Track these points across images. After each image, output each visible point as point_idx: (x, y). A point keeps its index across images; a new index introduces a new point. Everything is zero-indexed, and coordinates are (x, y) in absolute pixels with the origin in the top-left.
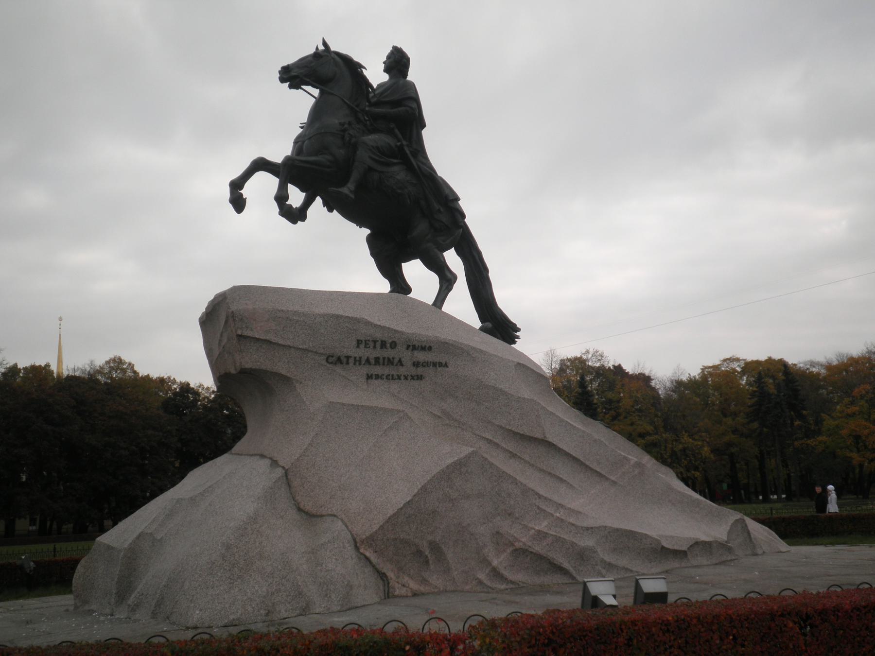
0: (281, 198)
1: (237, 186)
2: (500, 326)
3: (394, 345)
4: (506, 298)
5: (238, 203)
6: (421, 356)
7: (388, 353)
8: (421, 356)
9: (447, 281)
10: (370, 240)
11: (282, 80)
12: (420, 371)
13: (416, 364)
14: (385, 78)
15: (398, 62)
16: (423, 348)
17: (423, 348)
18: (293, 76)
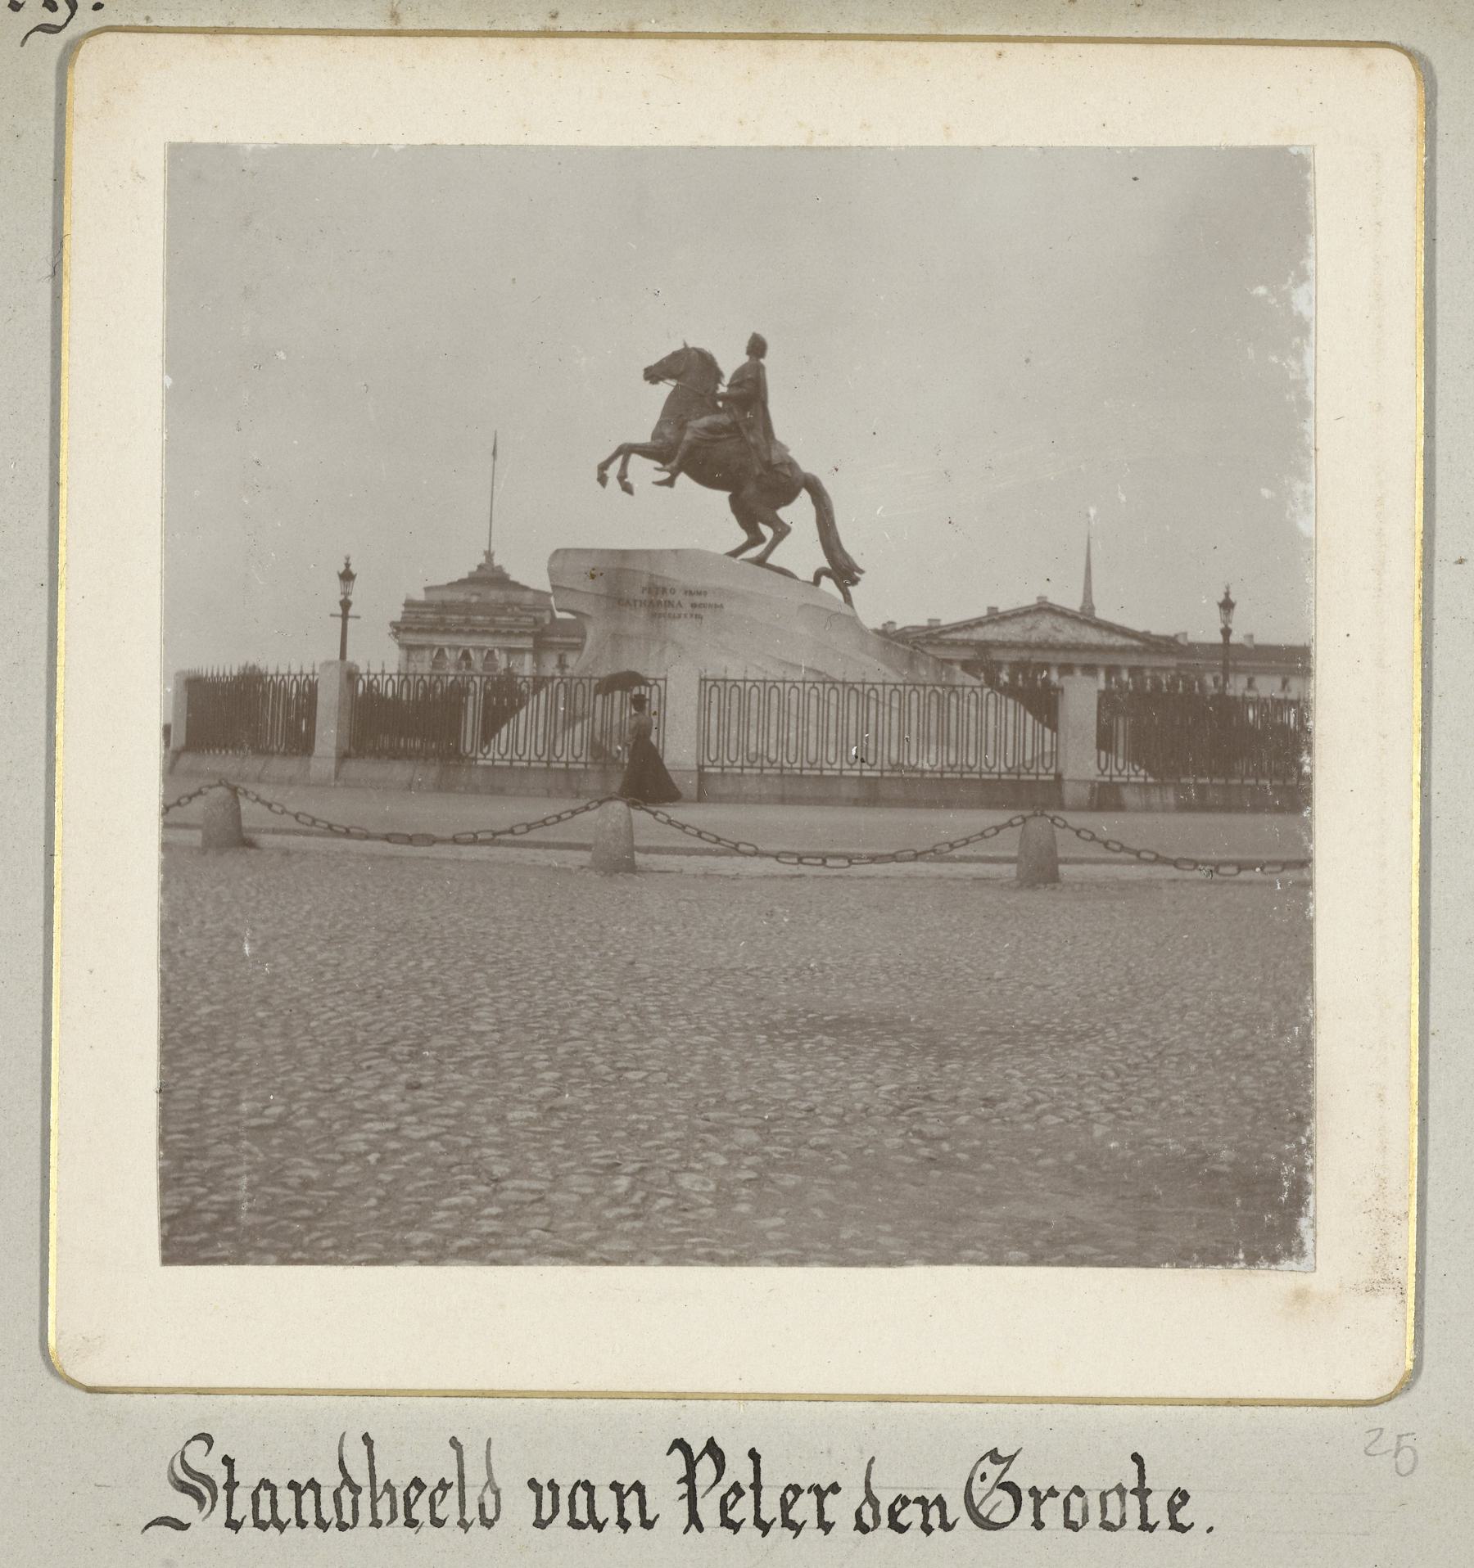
0: (622, 477)
1: (604, 467)
2: (843, 571)
3: (673, 591)
4: (852, 544)
5: (603, 480)
6: (697, 600)
7: (670, 597)
8: (697, 600)
9: (782, 531)
10: (732, 500)
11: (646, 378)
12: (697, 611)
13: (694, 606)
14: (745, 359)
15: (757, 347)
16: (699, 593)
17: (699, 593)
18: (653, 375)
